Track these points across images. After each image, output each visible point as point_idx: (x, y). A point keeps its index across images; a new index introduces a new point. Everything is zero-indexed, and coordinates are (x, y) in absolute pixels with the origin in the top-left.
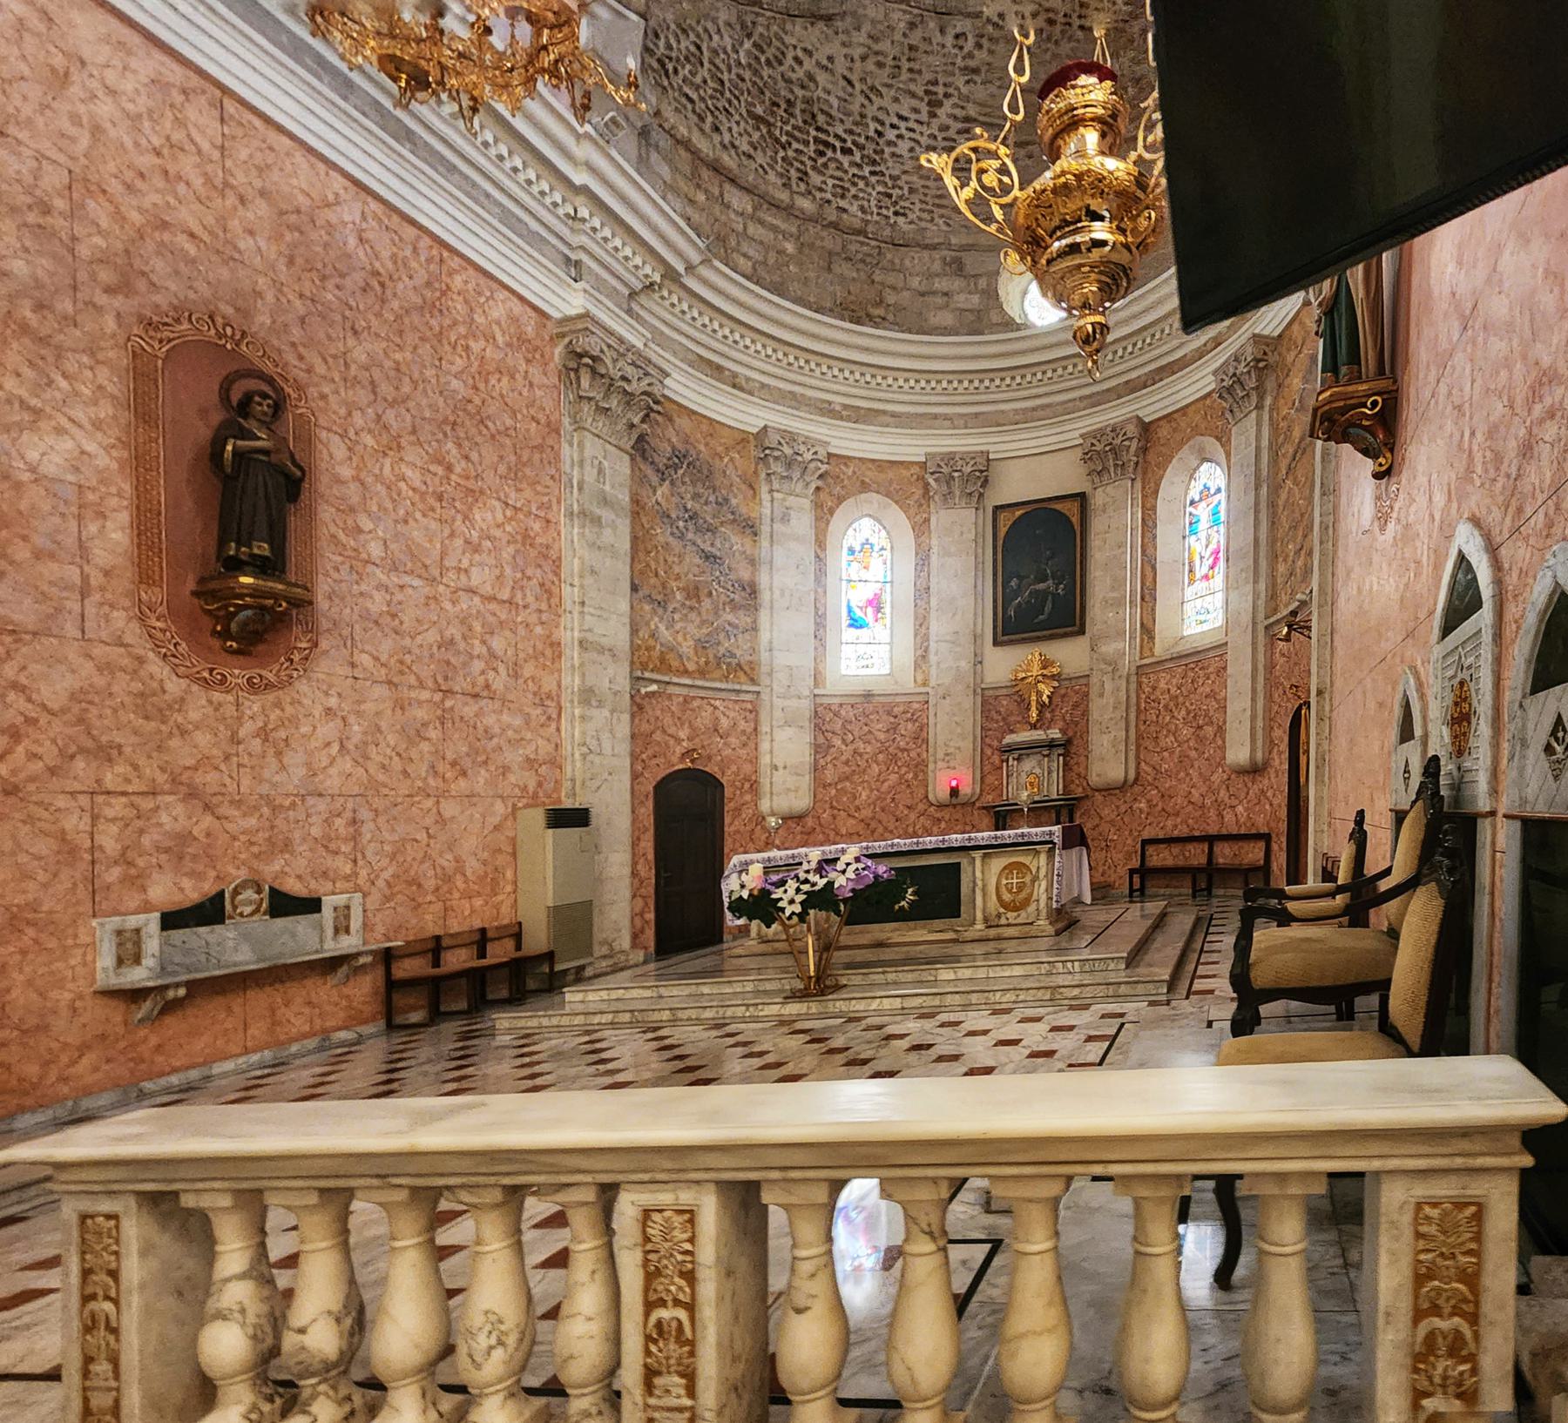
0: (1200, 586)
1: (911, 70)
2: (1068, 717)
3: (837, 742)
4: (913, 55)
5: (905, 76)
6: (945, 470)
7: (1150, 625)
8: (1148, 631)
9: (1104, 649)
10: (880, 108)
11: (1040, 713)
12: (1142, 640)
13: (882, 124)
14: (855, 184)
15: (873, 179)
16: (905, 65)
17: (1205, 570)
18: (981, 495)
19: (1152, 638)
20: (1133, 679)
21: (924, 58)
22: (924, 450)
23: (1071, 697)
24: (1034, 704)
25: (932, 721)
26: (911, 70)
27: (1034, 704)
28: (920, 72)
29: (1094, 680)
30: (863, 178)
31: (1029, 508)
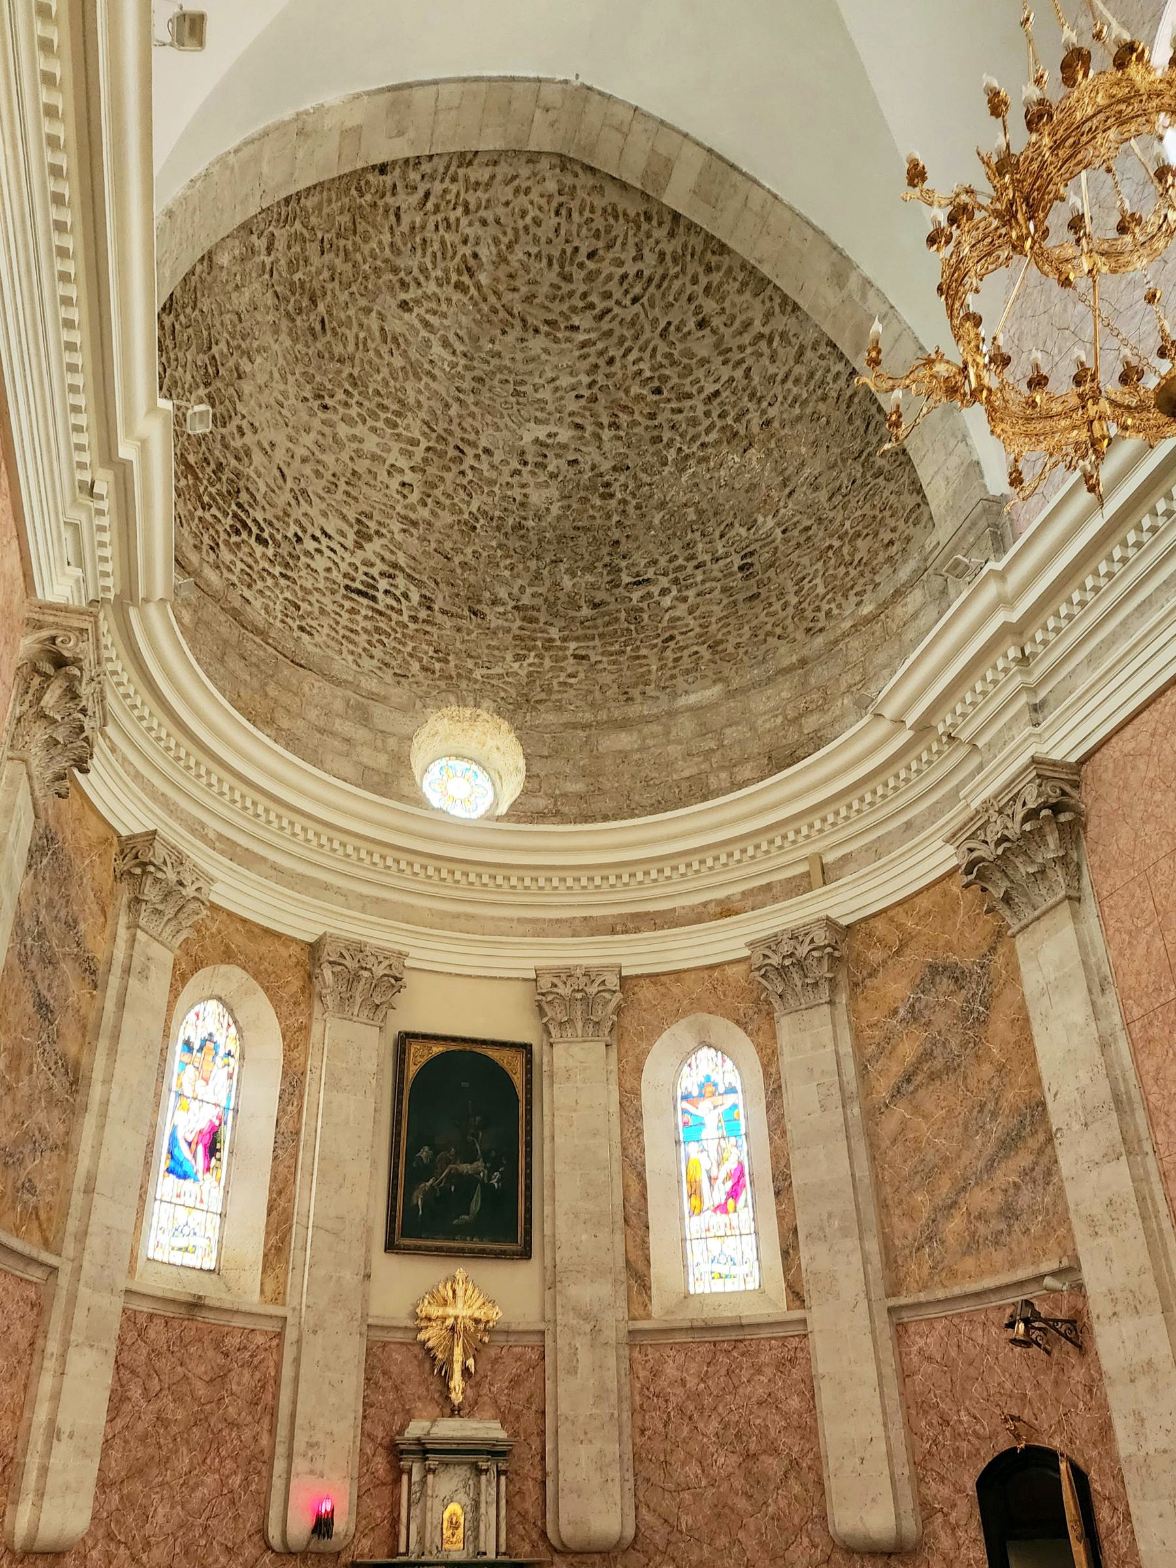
1: (347, 494)
4: (354, 480)
5: (339, 495)
10: (305, 514)
13: (305, 531)
14: (263, 579)
15: (283, 582)
16: (342, 486)
21: (365, 488)
23: (515, 1365)
25: (287, 1372)
26: (347, 494)
28: (355, 498)
30: (274, 576)
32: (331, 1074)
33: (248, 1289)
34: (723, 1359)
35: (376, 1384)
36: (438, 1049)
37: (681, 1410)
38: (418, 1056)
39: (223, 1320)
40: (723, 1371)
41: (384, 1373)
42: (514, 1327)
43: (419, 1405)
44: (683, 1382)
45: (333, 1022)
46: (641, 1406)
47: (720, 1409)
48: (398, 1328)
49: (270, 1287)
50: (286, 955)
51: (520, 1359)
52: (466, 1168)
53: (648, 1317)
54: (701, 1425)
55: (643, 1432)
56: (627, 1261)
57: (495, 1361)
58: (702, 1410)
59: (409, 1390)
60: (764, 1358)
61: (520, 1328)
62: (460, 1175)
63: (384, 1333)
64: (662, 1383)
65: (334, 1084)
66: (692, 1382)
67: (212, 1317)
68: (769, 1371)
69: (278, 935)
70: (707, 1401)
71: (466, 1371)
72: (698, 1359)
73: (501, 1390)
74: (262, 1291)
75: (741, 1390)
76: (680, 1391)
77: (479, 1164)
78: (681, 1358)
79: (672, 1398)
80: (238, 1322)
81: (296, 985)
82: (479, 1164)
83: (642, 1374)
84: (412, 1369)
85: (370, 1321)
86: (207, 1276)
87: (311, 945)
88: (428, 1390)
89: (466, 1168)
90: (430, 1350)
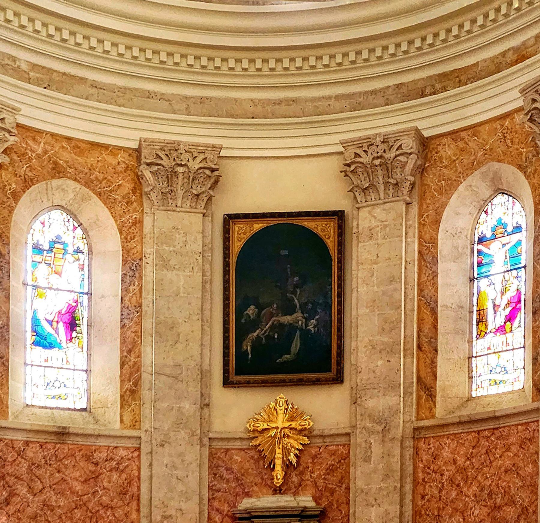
0: (493, 340)
2: (321, 483)
3: (22, 490)
6: (165, 162)
7: (428, 380)
8: (426, 388)
9: (370, 403)
11: (286, 477)
12: (419, 398)
17: (500, 320)
18: (210, 199)
19: (431, 395)
20: (409, 443)
22: (137, 135)
24: (278, 462)
27: (278, 462)
29: (359, 439)
31: (273, 222)
32: (159, 256)
33: (112, 419)
34: (483, 442)
35: (221, 477)
36: (258, 226)
37: (451, 480)
38: (241, 234)
39: (89, 442)
40: (484, 451)
41: (227, 469)
42: (327, 432)
43: (256, 488)
44: (455, 461)
45: (160, 215)
46: (423, 480)
47: (479, 478)
48: (235, 439)
49: (127, 418)
50: (115, 162)
51: (334, 454)
52: (287, 319)
53: (433, 417)
54: (465, 489)
55: (423, 497)
56: (419, 379)
57: (315, 457)
58: (466, 479)
59: (248, 479)
60: (513, 439)
61: (332, 433)
62: (281, 325)
63: (226, 443)
64: (439, 463)
65: (164, 263)
66: (461, 461)
67: (80, 441)
68: (514, 449)
69: (106, 147)
70: (471, 472)
71: (288, 466)
72: (467, 444)
73: (319, 476)
74: (122, 421)
75: (494, 464)
76: (452, 468)
77: (298, 315)
78: (454, 445)
79: (446, 473)
80: (102, 442)
81: (127, 187)
82: (298, 315)
83: (425, 458)
84: (249, 465)
85: (211, 435)
86: (78, 413)
87: (136, 150)
88: (262, 479)
89: (287, 319)
90: (260, 451)
